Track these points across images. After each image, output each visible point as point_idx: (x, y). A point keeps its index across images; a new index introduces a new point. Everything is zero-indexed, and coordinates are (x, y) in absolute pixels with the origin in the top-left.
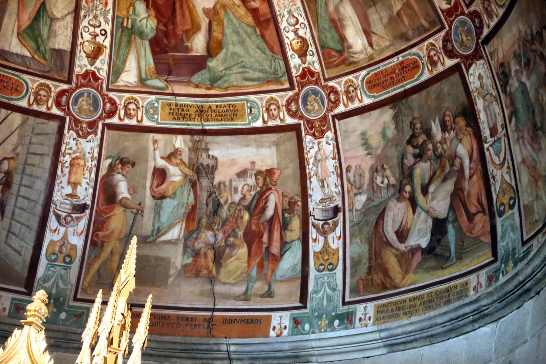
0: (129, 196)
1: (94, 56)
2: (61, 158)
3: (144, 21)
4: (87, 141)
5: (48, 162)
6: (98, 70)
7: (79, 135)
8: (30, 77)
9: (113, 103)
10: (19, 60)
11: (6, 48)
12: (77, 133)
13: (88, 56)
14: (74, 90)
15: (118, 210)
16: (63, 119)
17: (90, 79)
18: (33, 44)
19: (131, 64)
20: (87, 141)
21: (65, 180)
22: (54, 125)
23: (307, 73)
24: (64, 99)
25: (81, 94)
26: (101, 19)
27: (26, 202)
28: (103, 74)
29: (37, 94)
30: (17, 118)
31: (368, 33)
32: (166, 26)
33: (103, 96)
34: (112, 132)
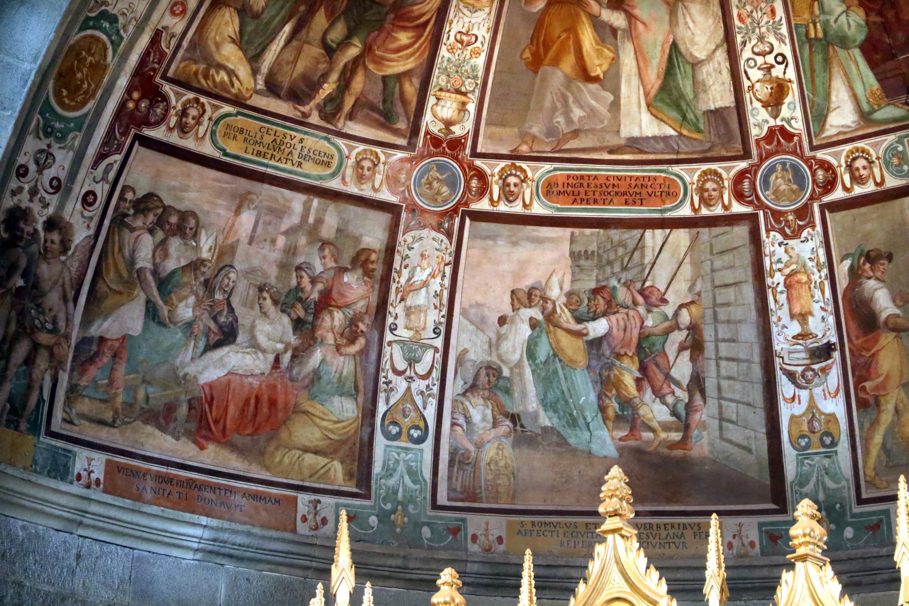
0: (898, 311)
1: (774, 102)
2: (769, 281)
3: (843, 17)
4: (802, 242)
5: (749, 292)
6: (788, 122)
7: (786, 236)
8: (868, 141)
9: (826, 166)
10: (661, 146)
11: (636, 133)
12: (782, 232)
13: (765, 105)
14: (758, 166)
15: (887, 340)
16: (753, 218)
17: (779, 141)
18: (674, 114)
19: (840, 95)
20: (802, 242)
21: (784, 313)
22: (741, 232)
24: (746, 184)
25: (772, 170)
26: (772, 39)
27: (733, 365)
28: (798, 126)
29: (701, 190)
30: (682, 237)
32: (880, 14)
33: (806, 161)
34: (839, 215)
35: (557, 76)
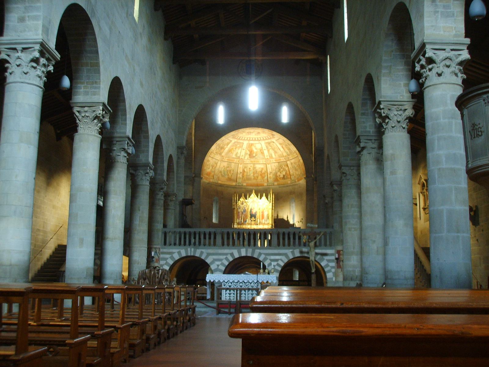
1: (243, 156)
23: (267, 159)
30: (234, 164)
31: (275, 155)
35: (230, 153)
